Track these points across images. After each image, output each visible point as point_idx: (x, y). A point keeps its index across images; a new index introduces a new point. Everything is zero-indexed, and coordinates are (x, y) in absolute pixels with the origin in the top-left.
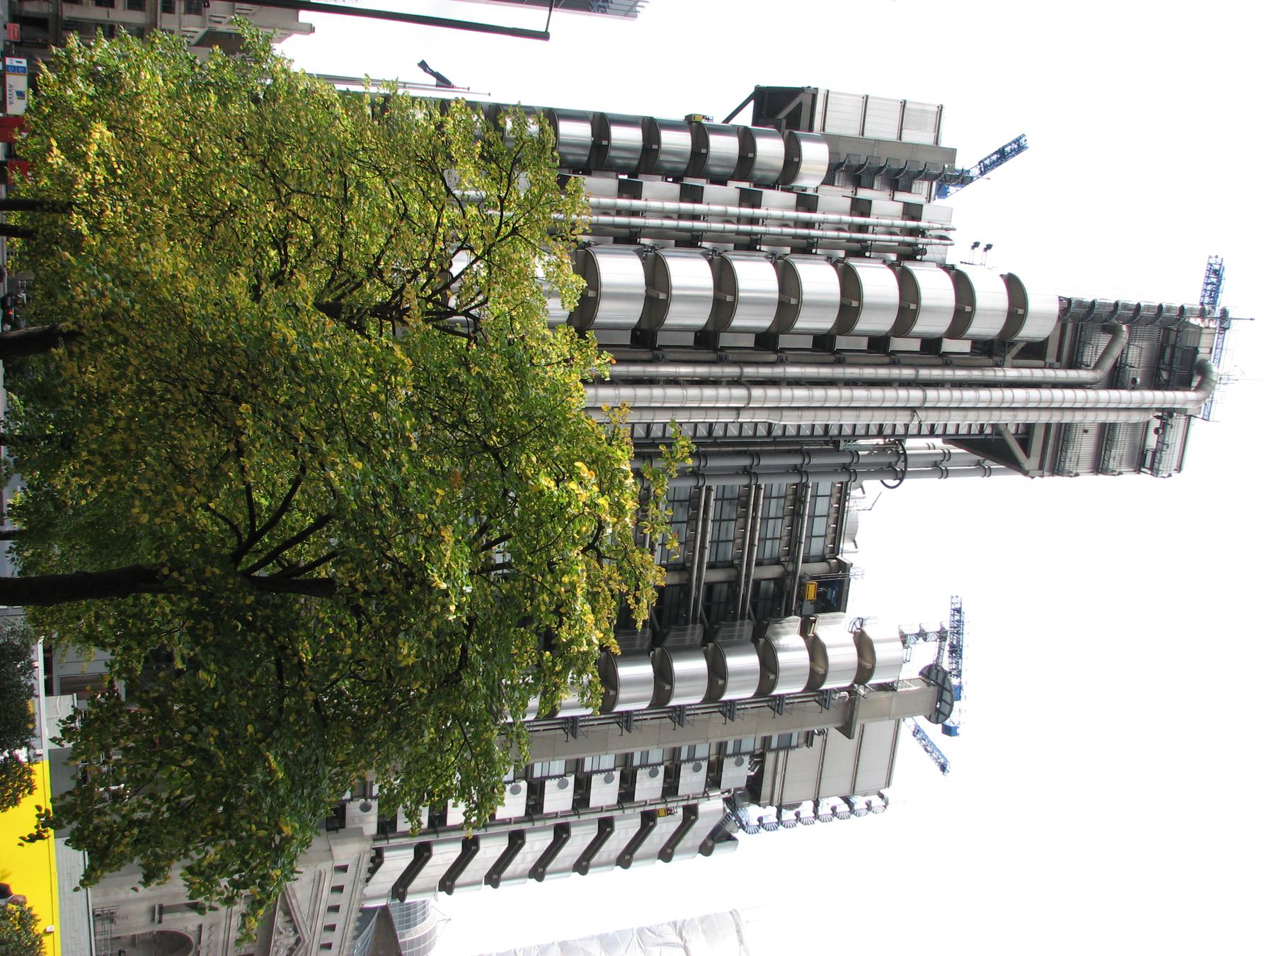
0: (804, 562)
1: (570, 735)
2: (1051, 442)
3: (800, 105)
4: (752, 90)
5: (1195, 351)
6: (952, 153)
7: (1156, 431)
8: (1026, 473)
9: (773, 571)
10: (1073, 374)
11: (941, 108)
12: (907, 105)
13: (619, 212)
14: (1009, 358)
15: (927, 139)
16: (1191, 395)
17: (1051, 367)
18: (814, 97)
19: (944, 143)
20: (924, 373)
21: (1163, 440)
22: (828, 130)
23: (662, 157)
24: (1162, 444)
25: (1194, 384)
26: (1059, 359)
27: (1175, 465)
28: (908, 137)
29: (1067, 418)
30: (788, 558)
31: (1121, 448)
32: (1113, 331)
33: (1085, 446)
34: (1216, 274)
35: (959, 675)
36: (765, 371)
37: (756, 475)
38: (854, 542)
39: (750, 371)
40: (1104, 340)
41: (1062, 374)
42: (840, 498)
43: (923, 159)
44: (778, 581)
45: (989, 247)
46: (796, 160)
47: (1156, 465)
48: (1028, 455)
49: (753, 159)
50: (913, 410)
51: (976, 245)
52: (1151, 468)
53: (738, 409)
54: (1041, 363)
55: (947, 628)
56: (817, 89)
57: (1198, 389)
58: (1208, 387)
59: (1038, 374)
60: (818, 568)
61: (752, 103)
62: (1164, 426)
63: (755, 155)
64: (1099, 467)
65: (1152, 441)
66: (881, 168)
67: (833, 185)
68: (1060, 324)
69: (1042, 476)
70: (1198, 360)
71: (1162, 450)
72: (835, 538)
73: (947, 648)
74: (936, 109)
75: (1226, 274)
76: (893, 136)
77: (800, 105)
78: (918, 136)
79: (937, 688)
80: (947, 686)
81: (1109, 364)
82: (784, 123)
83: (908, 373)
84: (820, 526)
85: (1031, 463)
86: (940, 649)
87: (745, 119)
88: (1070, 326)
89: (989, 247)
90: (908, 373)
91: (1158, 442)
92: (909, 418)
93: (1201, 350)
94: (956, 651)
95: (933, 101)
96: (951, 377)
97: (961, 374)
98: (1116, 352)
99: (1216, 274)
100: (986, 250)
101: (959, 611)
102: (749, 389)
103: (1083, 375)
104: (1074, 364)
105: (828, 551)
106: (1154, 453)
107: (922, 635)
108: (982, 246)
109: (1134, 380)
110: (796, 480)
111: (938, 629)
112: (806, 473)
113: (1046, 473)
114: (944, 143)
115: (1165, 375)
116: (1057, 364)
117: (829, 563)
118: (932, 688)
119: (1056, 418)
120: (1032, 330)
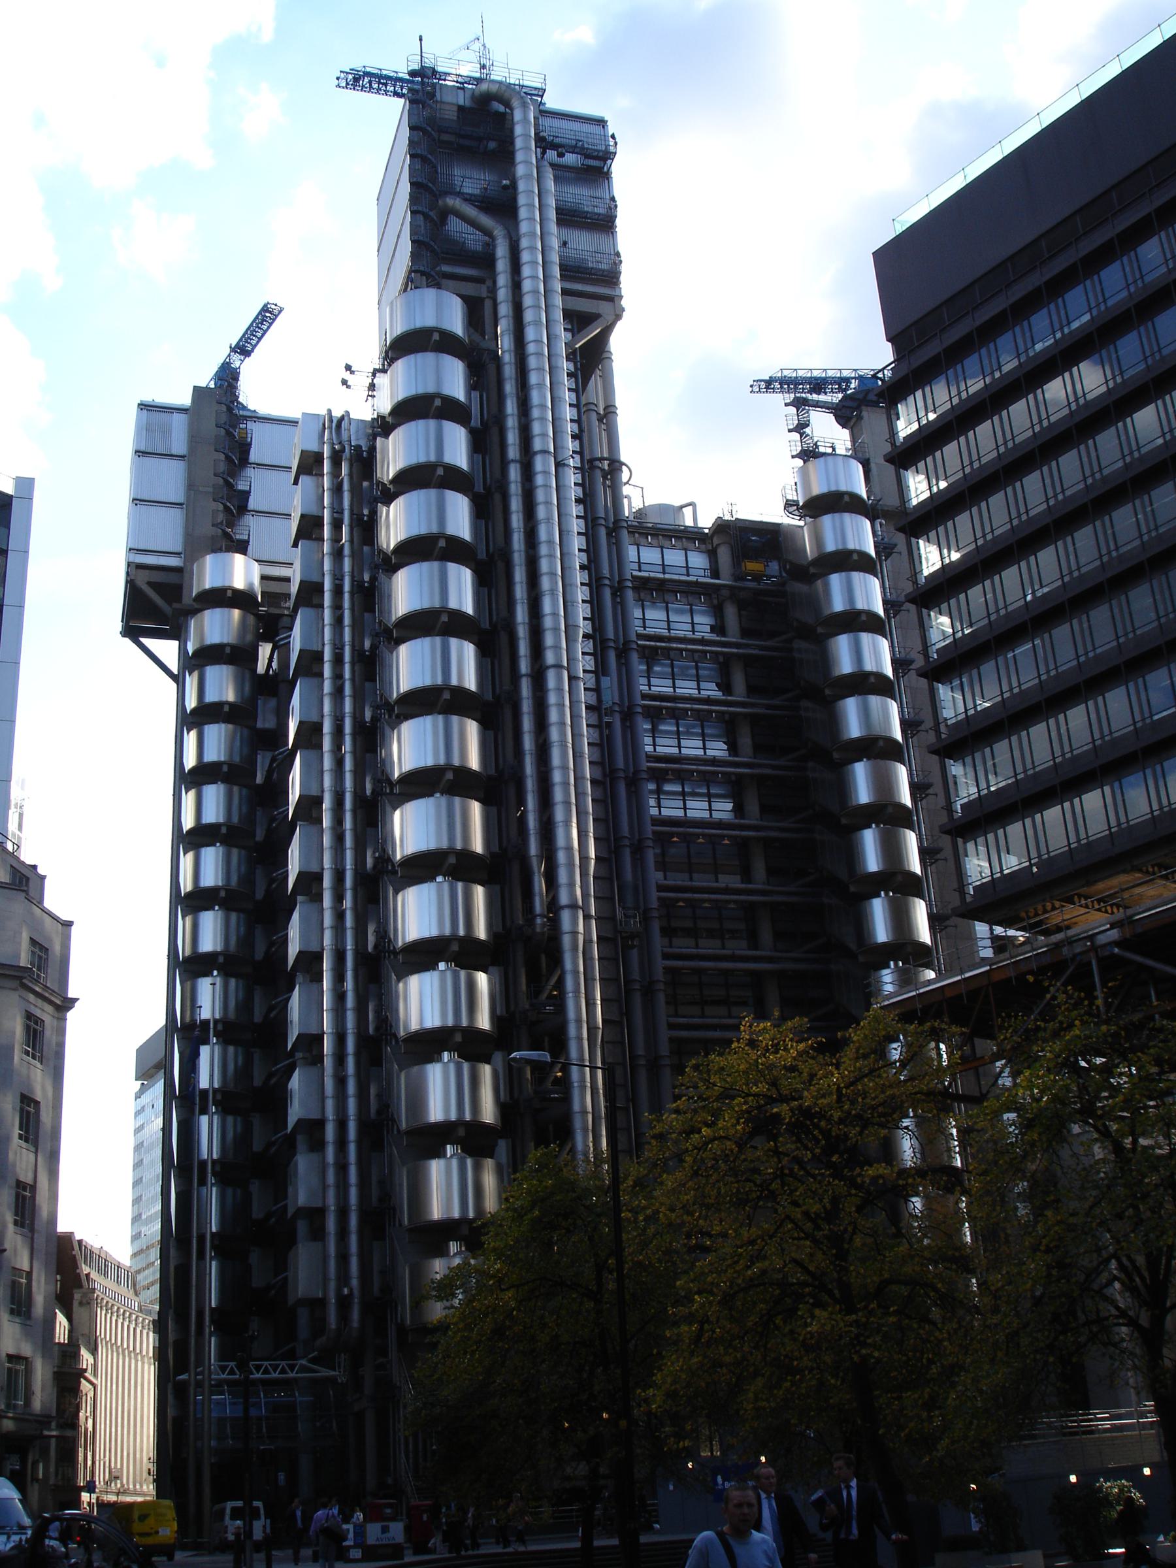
0: (718, 578)
1: (938, 856)
2: (579, 287)
3: (149, 583)
4: (127, 640)
5: (461, 109)
6: (198, 391)
7: (561, 155)
8: (618, 317)
9: (731, 612)
10: (502, 265)
11: (143, 406)
12: (143, 449)
13: (338, 821)
14: (484, 345)
15: (179, 424)
16: (518, 115)
17: (493, 290)
18: (140, 567)
19: (185, 400)
20: (513, 452)
21: (572, 147)
22: (179, 548)
23: (237, 759)
24: (574, 149)
25: (501, 108)
26: (479, 281)
27: (596, 129)
28: (179, 444)
29: (556, 271)
30: (714, 596)
31: (579, 195)
32: (445, 213)
33: (583, 243)
34: (359, 80)
35: (847, 380)
36: (523, 648)
37: (627, 642)
38: (682, 507)
39: (524, 666)
40: (455, 226)
41: (503, 280)
42: (639, 533)
43: (209, 427)
44: (742, 606)
45: (348, 368)
46: (229, 593)
47: (601, 154)
49: (232, 646)
50: (559, 465)
53: (570, 678)
54: (488, 304)
55: (790, 397)
56: (129, 564)
57: (507, 104)
58: (507, 95)
59: (504, 309)
60: (724, 555)
61: (147, 642)
62: (554, 146)
63: (228, 645)
64: (605, 223)
65: (570, 159)
66: (227, 483)
67: (247, 542)
68: (444, 282)
69: (621, 297)
70: (474, 106)
71: (583, 148)
72: (688, 539)
73: (815, 397)
75: (358, 64)
77: (149, 583)
79: (863, 408)
80: (861, 396)
81: (486, 220)
82: (176, 605)
83: (514, 473)
84: (674, 557)
86: (817, 405)
87: (167, 650)
88: (446, 268)
89: (348, 368)
90: (514, 473)
91: (573, 153)
92: (566, 469)
93: (461, 102)
94: (818, 385)
95: (130, 416)
96: (516, 418)
97: (511, 407)
98: (471, 211)
99: (359, 80)
100: (352, 372)
101: (769, 385)
102: (548, 667)
104: (487, 261)
105: (703, 547)
106: (587, 156)
107: (800, 428)
108: (347, 376)
109: (505, 187)
110: (630, 595)
111: (793, 410)
112: (621, 581)
114: (185, 400)
115: (492, 145)
116: (489, 283)
117: (718, 545)
118: (864, 414)
119: (557, 286)
120: (455, 322)
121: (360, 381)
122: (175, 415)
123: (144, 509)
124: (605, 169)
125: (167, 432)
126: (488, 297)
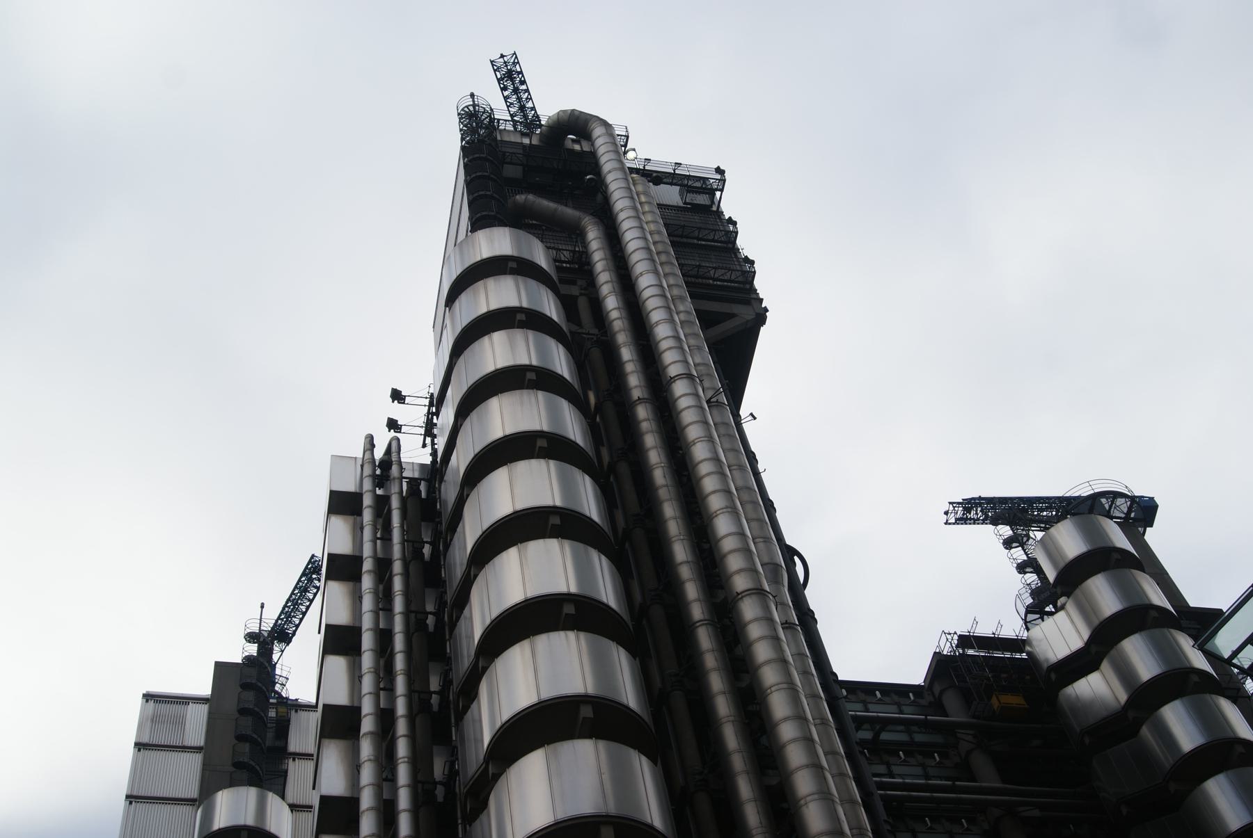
6: (221, 669)
8: (760, 317)
11: (148, 697)
12: (145, 740)
19: (206, 690)
45: (397, 396)
48: (732, 316)
51: (393, 425)
52: (711, 192)
70: (541, 144)
74: (151, 703)
76: (196, 760)
78: (195, 726)
85: (745, 313)
89: (397, 396)
91: (671, 184)
103: (594, 237)
113: (754, 296)
117: (942, 692)
121: (413, 415)
122: (192, 707)
123: (141, 807)
124: (714, 208)
125: (180, 722)
126: (581, 294)
